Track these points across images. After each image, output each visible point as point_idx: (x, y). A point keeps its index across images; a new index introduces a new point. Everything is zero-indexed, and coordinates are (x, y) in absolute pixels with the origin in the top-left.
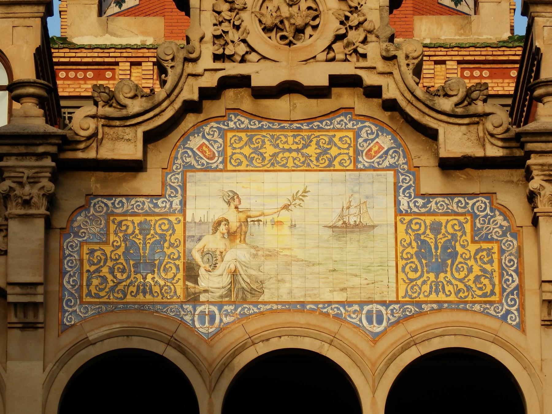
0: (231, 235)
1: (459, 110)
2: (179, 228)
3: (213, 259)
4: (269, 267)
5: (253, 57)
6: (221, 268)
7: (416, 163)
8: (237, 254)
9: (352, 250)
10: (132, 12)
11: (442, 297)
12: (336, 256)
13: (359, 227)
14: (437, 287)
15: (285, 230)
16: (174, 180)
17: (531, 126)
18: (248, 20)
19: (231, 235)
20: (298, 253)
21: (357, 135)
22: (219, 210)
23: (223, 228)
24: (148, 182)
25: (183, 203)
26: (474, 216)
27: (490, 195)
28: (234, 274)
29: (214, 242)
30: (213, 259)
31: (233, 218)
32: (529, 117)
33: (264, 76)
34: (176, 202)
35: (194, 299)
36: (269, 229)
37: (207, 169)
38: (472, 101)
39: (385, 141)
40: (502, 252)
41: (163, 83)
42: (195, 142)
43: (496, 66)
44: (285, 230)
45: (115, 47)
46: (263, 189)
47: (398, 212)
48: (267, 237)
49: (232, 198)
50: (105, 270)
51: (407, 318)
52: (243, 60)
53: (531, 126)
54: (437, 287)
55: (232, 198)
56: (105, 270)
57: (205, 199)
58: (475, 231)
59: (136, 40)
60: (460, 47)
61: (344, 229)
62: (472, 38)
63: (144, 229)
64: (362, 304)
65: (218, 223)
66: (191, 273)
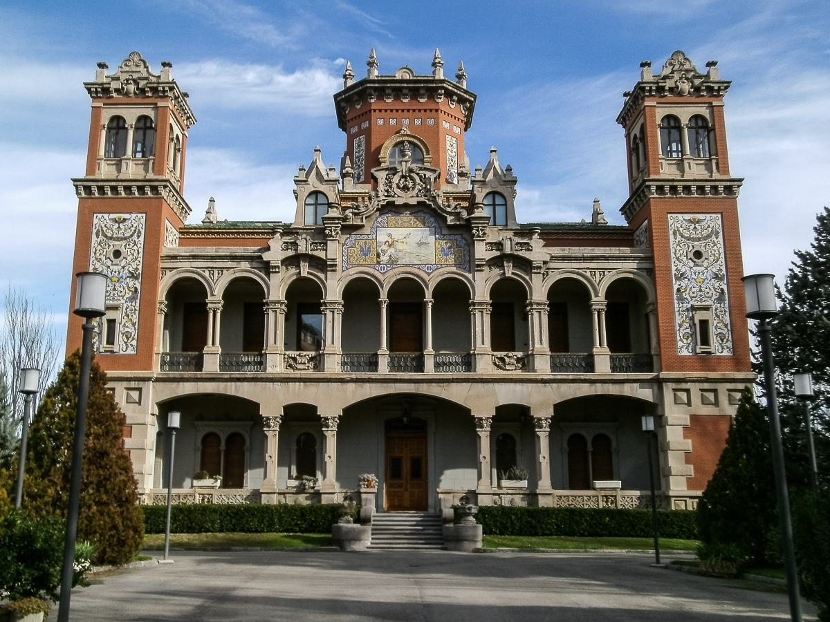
0: (390, 246)
1: (453, 211)
2: (375, 243)
3: (384, 252)
4: (400, 254)
5: (396, 196)
6: (386, 254)
7: (441, 225)
8: (391, 251)
9: (423, 250)
10: (361, 183)
11: (448, 263)
12: (419, 251)
13: (425, 243)
14: (446, 260)
15: (405, 244)
16: (374, 230)
17: (473, 216)
18: (394, 186)
19: (390, 246)
20: (409, 251)
21: (425, 218)
22: (387, 238)
23: (387, 243)
24: (367, 231)
25: (376, 236)
26: (457, 240)
27: (462, 235)
28: (390, 256)
29: (385, 247)
30: (384, 252)
31: (390, 241)
32: (473, 212)
33: (399, 201)
34: (374, 237)
35: (379, 263)
36: (400, 244)
37: (383, 227)
38: (457, 209)
39: (432, 220)
40: (464, 250)
41: (371, 203)
42: (379, 219)
43: (464, 199)
44: (405, 244)
45: (357, 193)
46: (398, 233)
47: (436, 239)
48: (400, 246)
49: (390, 235)
50: (354, 255)
51: (437, 269)
52: (393, 197)
53: (473, 216)
54: (446, 260)
55: (390, 235)
56: (354, 255)
57: (382, 236)
58: (457, 245)
59: (363, 191)
60: (453, 193)
61: (420, 244)
62: (458, 191)
63: (366, 243)
64: (425, 265)
65: (386, 242)
66: (378, 256)
